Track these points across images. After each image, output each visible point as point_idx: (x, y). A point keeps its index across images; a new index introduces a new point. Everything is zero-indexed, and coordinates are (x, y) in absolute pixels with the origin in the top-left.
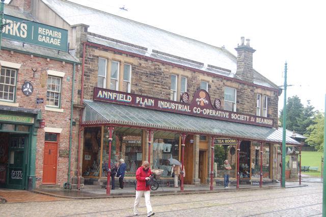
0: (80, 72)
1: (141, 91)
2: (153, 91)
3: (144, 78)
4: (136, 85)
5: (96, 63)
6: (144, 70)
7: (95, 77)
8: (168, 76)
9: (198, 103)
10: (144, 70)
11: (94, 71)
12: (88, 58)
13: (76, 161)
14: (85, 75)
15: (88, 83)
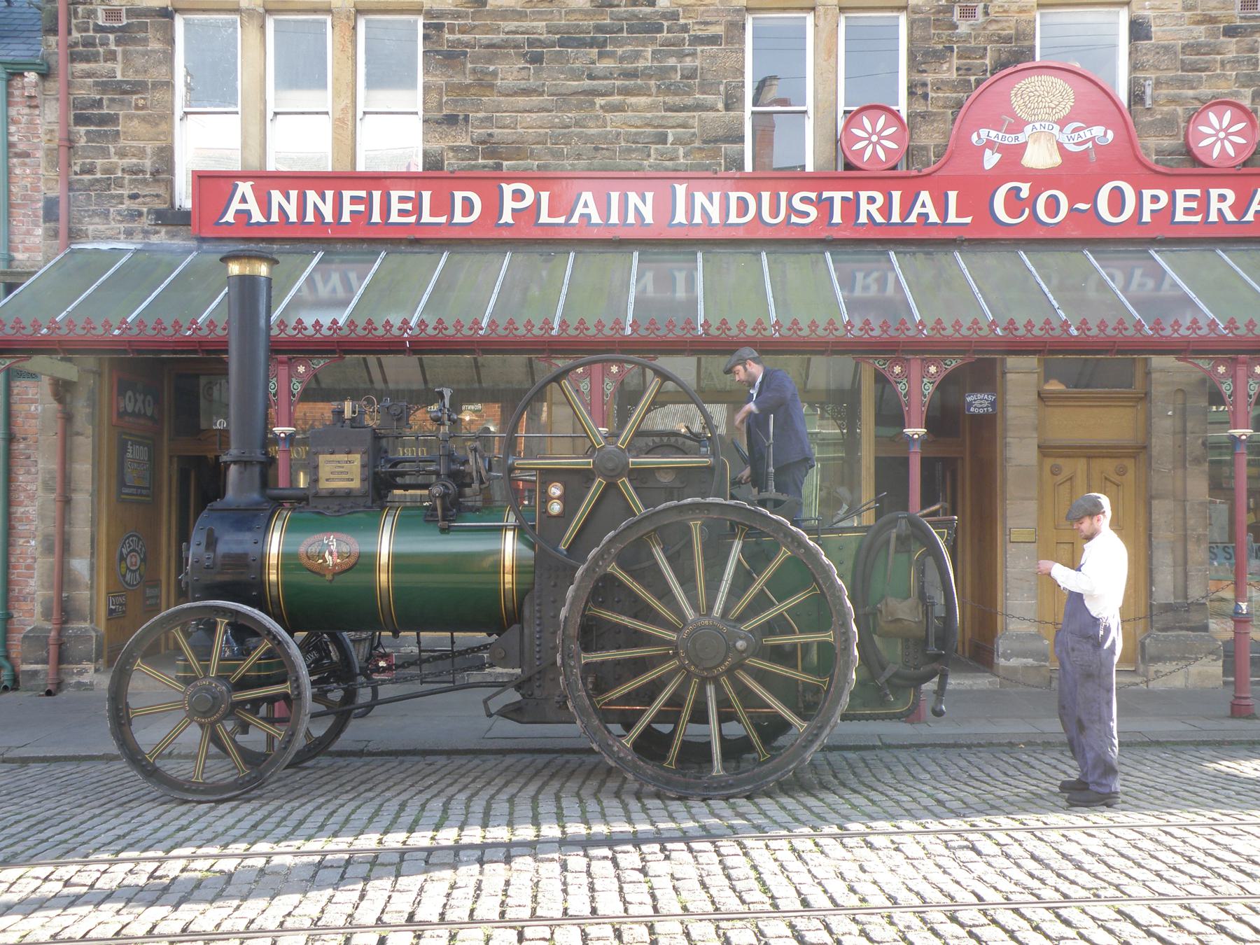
0: (50, 115)
1: (491, 148)
2: (588, 139)
3: (509, 72)
4: (451, 120)
5: (155, 45)
6: (512, 25)
7: (143, 119)
8: (718, 30)
9: (991, 160)
10: (512, 25)
11: (138, 87)
12: (99, 29)
13: (49, 550)
14: (81, 120)
15: (105, 153)
